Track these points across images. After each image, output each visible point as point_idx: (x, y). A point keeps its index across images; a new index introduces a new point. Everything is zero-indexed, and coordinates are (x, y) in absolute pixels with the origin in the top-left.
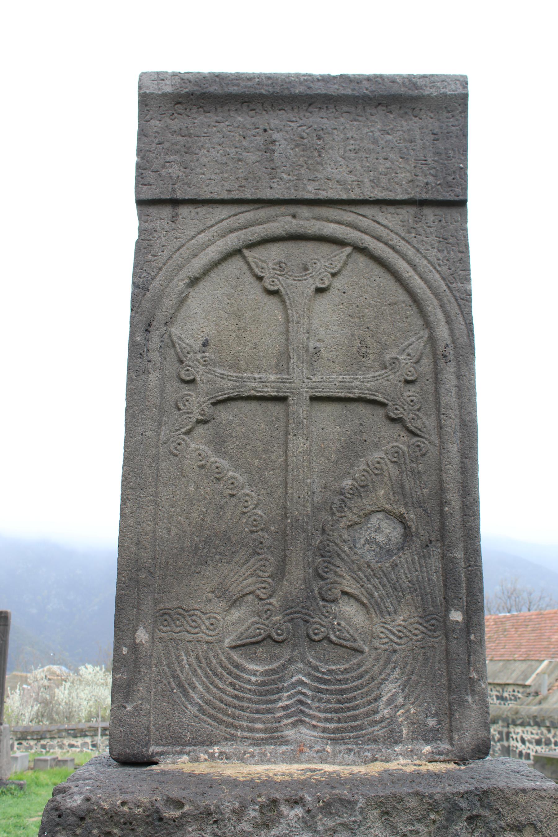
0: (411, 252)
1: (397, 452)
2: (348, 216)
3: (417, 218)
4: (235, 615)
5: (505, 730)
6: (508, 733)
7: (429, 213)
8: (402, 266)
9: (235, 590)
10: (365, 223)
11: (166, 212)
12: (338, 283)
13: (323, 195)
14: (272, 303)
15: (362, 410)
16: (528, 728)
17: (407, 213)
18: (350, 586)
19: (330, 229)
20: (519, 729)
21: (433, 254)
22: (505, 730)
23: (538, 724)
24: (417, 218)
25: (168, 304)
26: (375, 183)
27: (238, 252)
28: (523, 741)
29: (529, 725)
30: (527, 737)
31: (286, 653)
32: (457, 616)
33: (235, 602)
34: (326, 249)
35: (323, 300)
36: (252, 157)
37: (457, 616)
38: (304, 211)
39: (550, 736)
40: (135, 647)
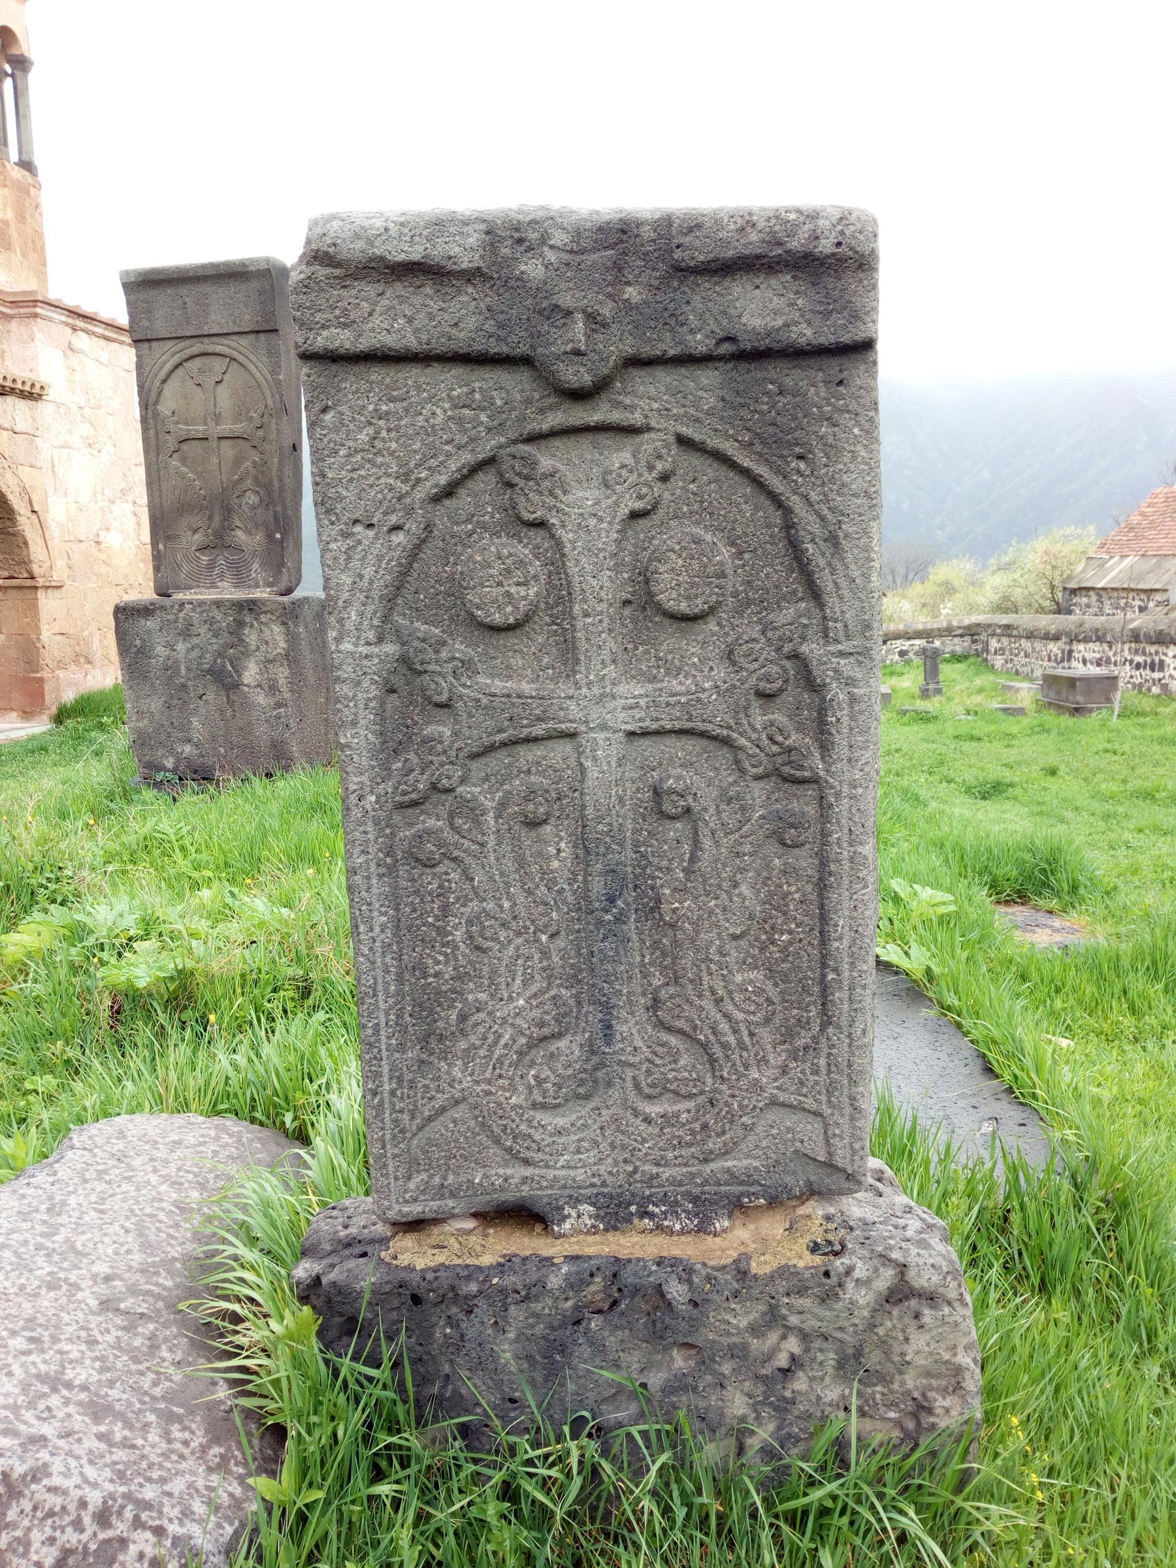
0: (254, 358)
1: (254, 462)
2: (226, 341)
3: (257, 340)
4: (196, 537)
5: (1067, 648)
6: (1071, 652)
7: (262, 337)
8: (251, 367)
9: (195, 526)
10: (234, 344)
11: (146, 345)
12: (226, 377)
13: (212, 331)
14: (198, 389)
15: (241, 441)
16: (1091, 645)
17: (251, 337)
18: (238, 523)
19: (219, 349)
20: (1081, 647)
21: (265, 359)
22: (1067, 648)
23: (1100, 639)
24: (257, 340)
25: (154, 394)
26: (234, 322)
27: (181, 364)
28: (1085, 662)
29: (1091, 641)
30: (1088, 656)
31: (216, 551)
32: (278, 536)
33: (195, 532)
34: (219, 359)
35: (221, 387)
36: (178, 313)
37: (278, 536)
38: (206, 340)
39: (1111, 654)
40: (159, 551)
